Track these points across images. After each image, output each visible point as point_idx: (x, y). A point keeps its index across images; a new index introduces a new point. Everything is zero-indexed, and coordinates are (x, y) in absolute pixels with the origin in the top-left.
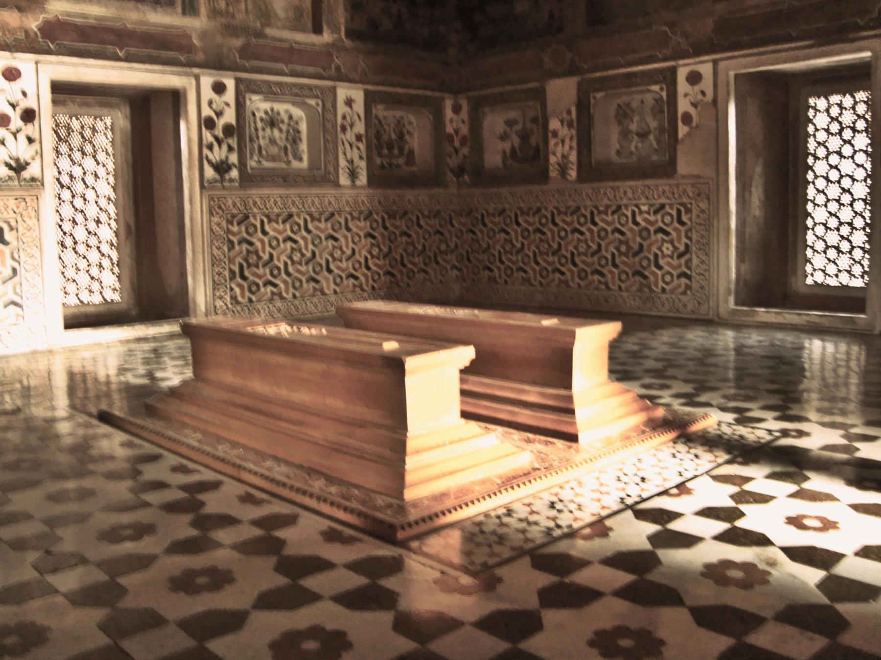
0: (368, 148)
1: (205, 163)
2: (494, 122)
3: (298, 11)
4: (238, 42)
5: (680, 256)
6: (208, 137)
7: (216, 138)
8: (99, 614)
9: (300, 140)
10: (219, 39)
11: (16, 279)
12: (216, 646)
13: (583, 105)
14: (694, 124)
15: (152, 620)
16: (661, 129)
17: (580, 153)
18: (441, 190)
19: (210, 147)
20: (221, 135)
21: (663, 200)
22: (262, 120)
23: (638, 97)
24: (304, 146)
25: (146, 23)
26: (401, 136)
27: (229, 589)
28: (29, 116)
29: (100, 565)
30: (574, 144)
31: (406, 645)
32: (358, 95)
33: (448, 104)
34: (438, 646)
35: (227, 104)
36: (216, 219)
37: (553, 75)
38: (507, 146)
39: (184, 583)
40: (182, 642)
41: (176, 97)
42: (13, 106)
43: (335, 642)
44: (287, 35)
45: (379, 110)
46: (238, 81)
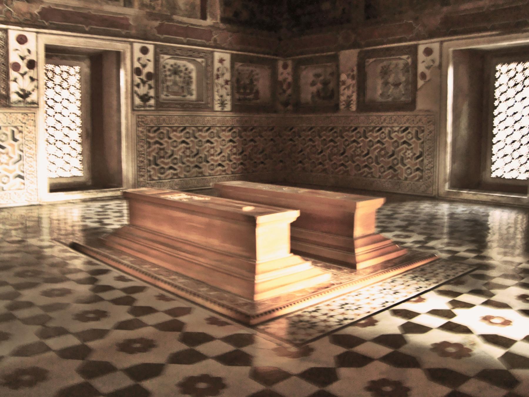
0: (232, 88)
1: (135, 95)
2: (308, 75)
3: (193, 6)
4: (157, 23)
5: (418, 158)
6: (137, 79)
7: (142, 80)
8: (77, 363)
9: (191, 82)
10: (145, 22)
11: (21, 162)
12: (148, 384)
13: (361, 66)
14: (428, 79)
15: (106, 368)
16: (407, 82)
17: (358, 95)
18: (274, 115)
19: (138, 86)
20: (145, 79)
21: (407, 125)
22: (169, 70)
23: (394, 62)
24: (194, 86)
25: (102, 11)
26: (252, 82)
27: (154, 350)
28: (32, 65)
29: (77, 335)
30: (355, 89)
31: (257, 387)
32: (227, 57)
33: (280, 63)
34: (280, 387)
35: (149, 60)
36: (140, 129)
37: (344, 48)
38: (314, 89)
39: (127, 347)
40: (127, 382)
41: (118, 56)
42: (23, 58)
43: (217, 384)
44: (185, 19)
45: (238, 65)
46: (156, 46)
